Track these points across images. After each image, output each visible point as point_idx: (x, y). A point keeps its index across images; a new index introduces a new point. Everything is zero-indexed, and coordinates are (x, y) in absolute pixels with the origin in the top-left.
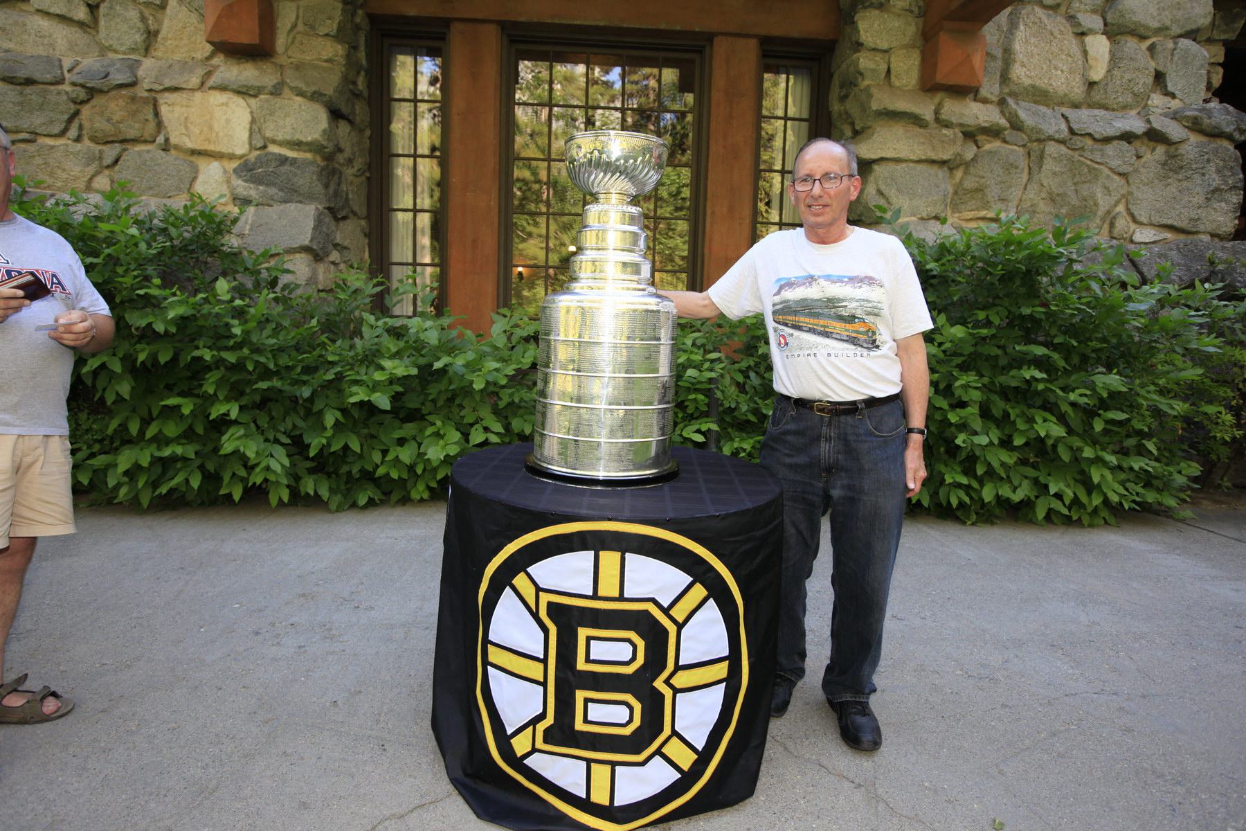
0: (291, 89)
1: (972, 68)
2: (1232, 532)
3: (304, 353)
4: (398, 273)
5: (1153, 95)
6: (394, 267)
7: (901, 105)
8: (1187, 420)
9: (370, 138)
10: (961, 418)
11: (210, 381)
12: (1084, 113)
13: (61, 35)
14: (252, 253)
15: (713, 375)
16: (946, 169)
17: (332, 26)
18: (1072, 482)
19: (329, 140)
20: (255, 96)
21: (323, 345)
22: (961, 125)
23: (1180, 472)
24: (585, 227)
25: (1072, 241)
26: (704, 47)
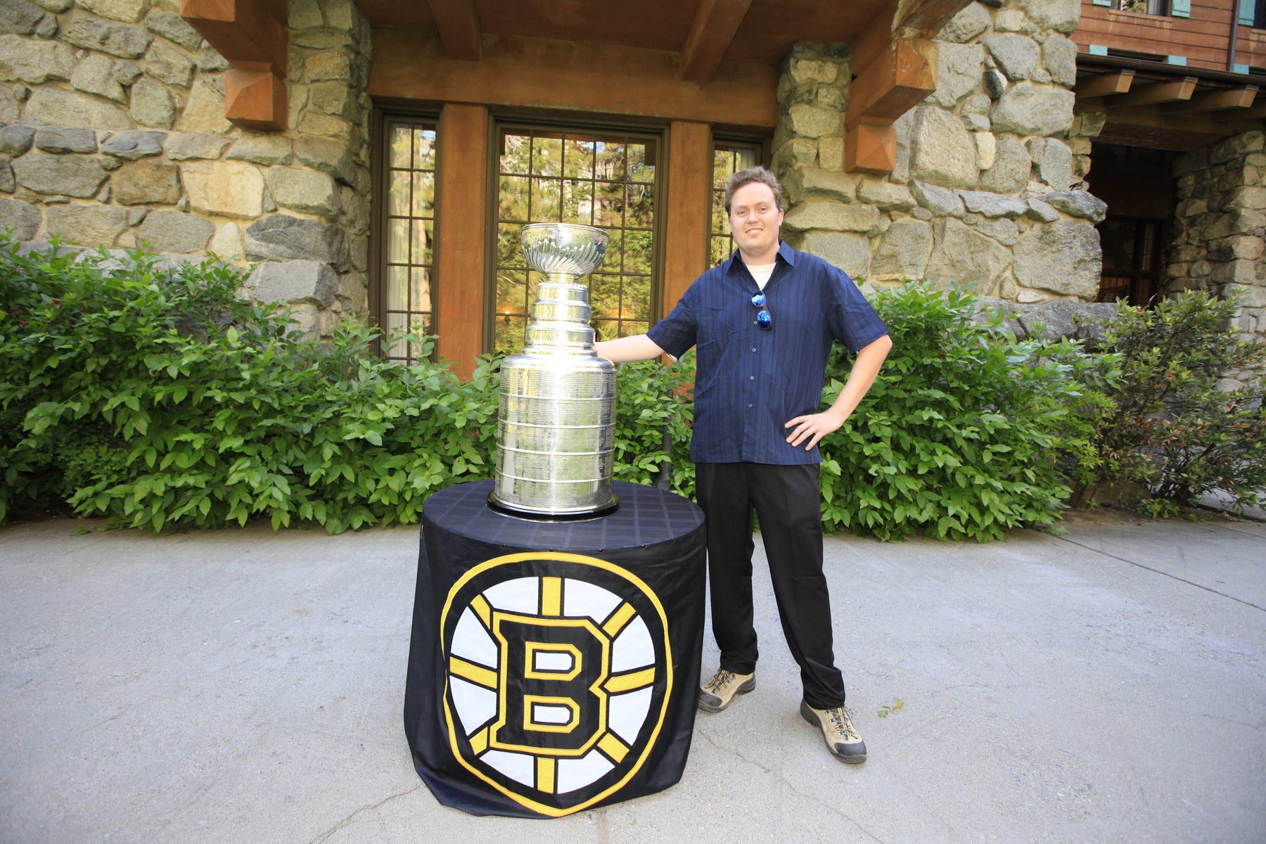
0: (300, 160)
1: (885, 155)
2: (1095, 544)
3: (306, 394)
4: (395, 321)
5: (1030, 182)
6: (391, 315)
7: (827, 184)
8: (1061, 451)
9: (371, 202)
10: (875, 451)
11: (221, 418)
12: (977, 195)
13: (97, 111)
14: (261, 303)
15: (665, 414)
17: (338, 107)
18: (967, 505)
19: (333, 204)
20: (268, 166)
21: (323, 387)
22: (878, 202)
23: (1054, 495)
24: (538, 300)
25: (965, 302)
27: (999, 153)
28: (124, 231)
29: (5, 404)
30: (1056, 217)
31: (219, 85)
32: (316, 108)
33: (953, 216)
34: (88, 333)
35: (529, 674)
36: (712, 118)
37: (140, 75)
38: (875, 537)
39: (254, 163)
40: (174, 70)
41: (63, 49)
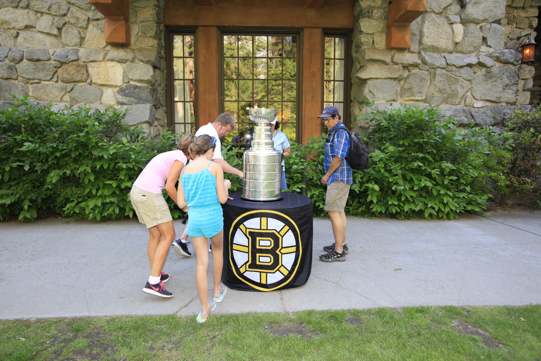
0: (138, 59)
1: (406, 41)
2: (501, 220)
4: (180, 129)
5: (482, 47)
7: (377, 57)
9: (166, 74)
10: (394, 180)
12: (454, 55)
13: (48, 40)
15: (303, 167)
16: (397, 81)
17: (153, 33)
19: (153, 79)
20: (125, 63)
22: (402, 64)
23: (480, 198)
26: (300, 32)
27: (465, 34)
28: (65, 94)
29: (39, 172)
30: (493, 64)
31: (100, 26)
32: (142, 34)
33: (440, 68)
34: (72, 142)
35: (258, 247)
36: (323, 26)
37: (66, 23)
38: (398, 219)
39: (118, 62)
40: (80, 20)
41: (31, 13)
